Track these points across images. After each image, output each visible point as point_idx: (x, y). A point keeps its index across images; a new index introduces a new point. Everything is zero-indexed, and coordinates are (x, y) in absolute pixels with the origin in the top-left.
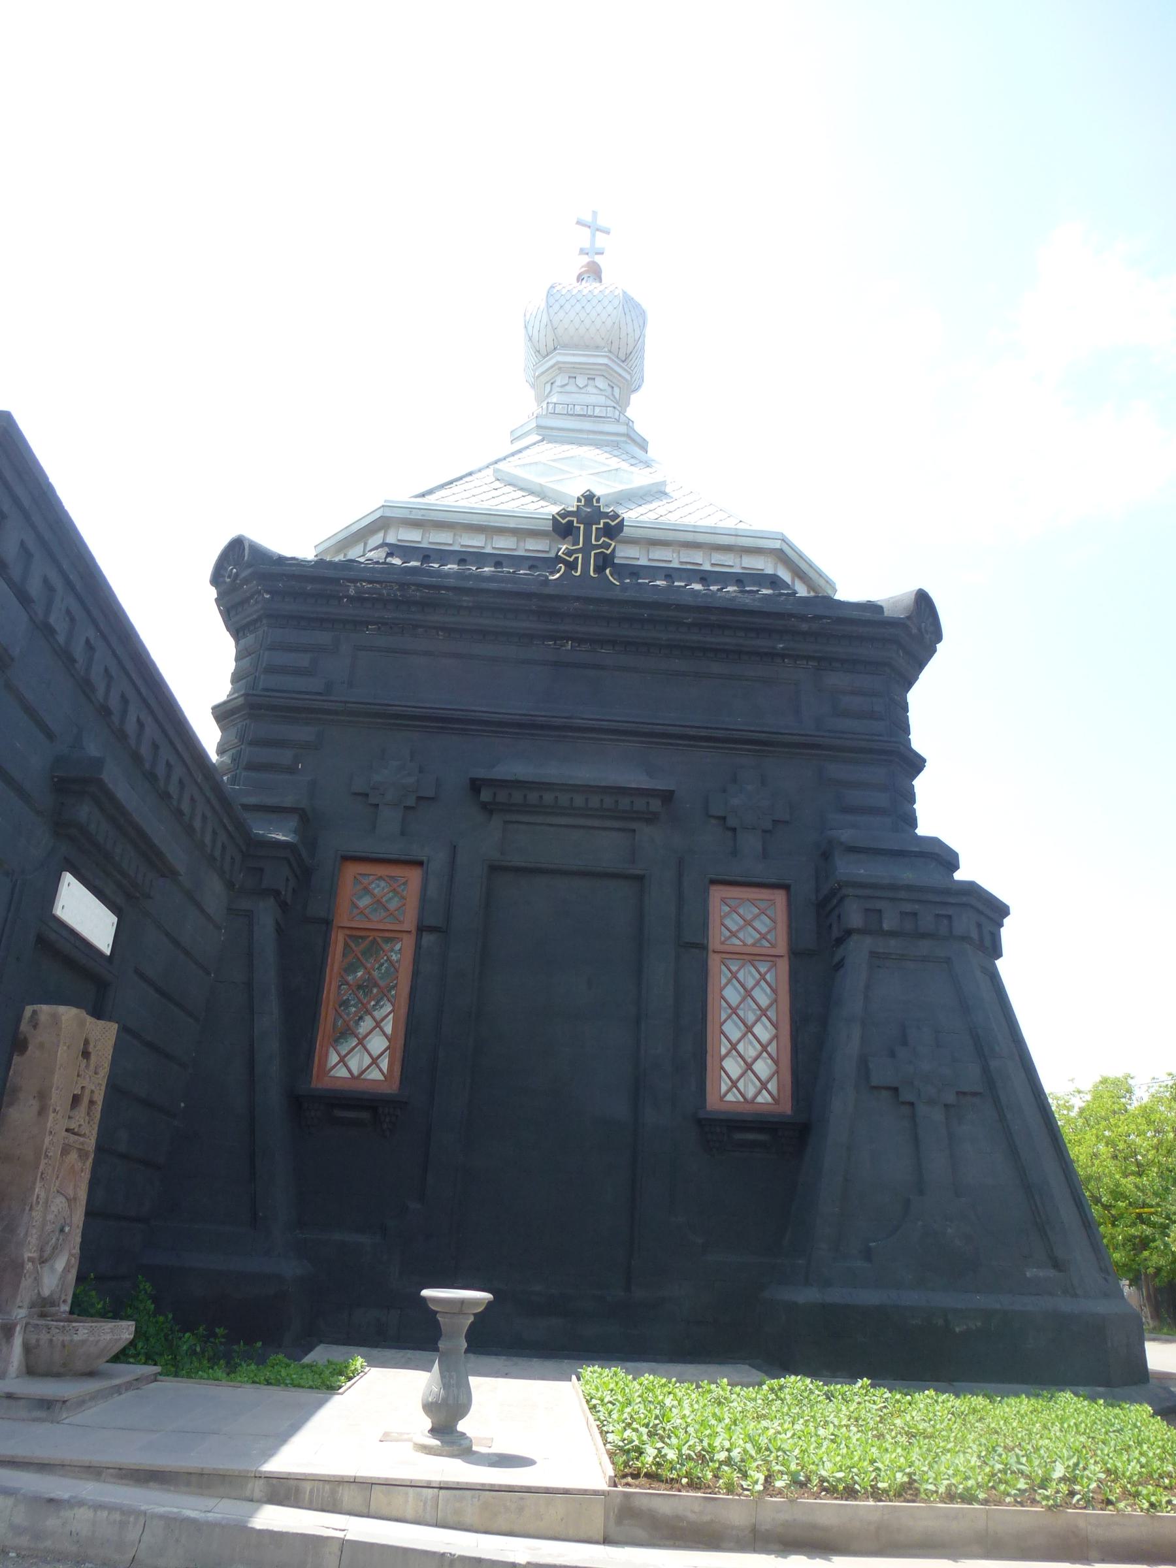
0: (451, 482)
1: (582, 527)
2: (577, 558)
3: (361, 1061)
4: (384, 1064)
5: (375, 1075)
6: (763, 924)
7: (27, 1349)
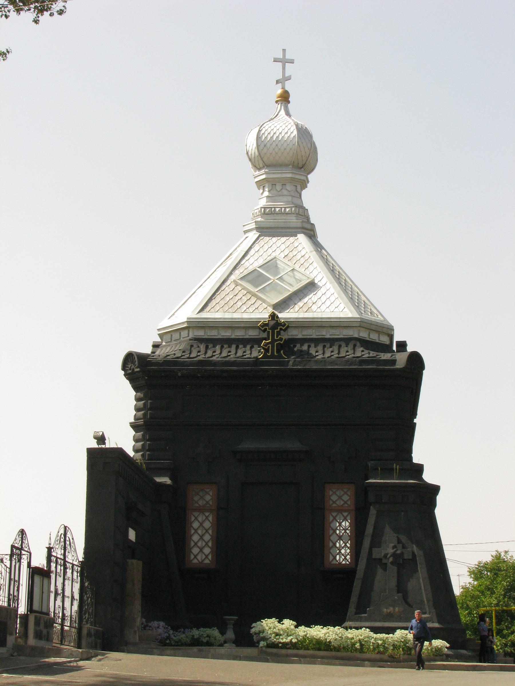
0: (214, 294)
1: (271, 331)
2: (269, 347)
3: (202, 557)
4: (210, 557)
5: (207, 561)
6: (346, 498)
7: (139, 637)
